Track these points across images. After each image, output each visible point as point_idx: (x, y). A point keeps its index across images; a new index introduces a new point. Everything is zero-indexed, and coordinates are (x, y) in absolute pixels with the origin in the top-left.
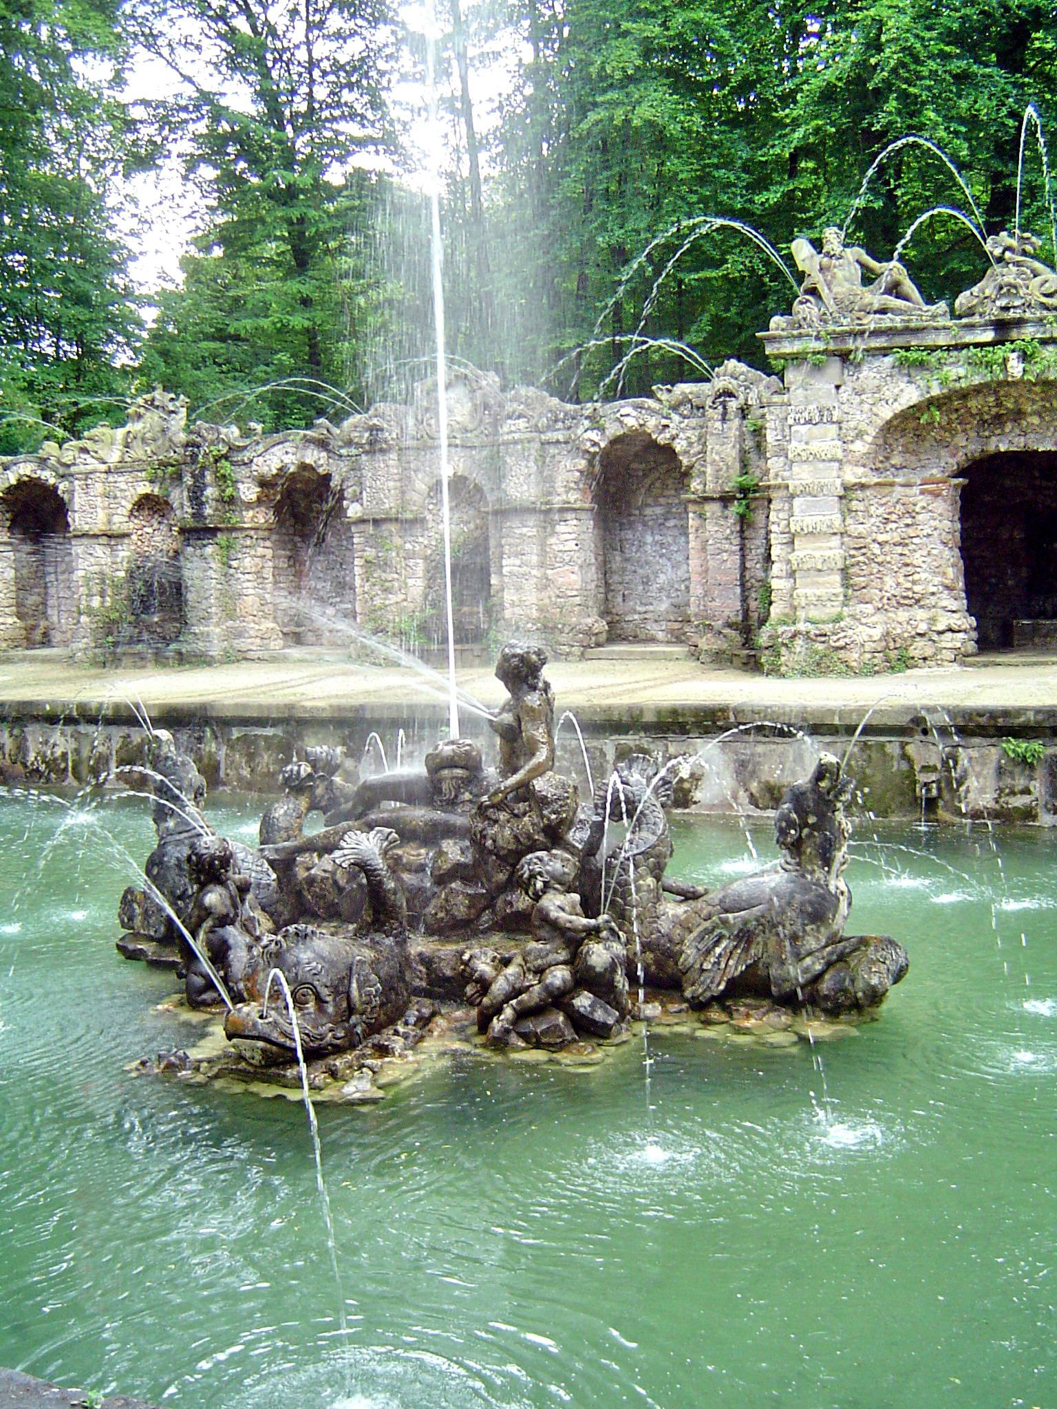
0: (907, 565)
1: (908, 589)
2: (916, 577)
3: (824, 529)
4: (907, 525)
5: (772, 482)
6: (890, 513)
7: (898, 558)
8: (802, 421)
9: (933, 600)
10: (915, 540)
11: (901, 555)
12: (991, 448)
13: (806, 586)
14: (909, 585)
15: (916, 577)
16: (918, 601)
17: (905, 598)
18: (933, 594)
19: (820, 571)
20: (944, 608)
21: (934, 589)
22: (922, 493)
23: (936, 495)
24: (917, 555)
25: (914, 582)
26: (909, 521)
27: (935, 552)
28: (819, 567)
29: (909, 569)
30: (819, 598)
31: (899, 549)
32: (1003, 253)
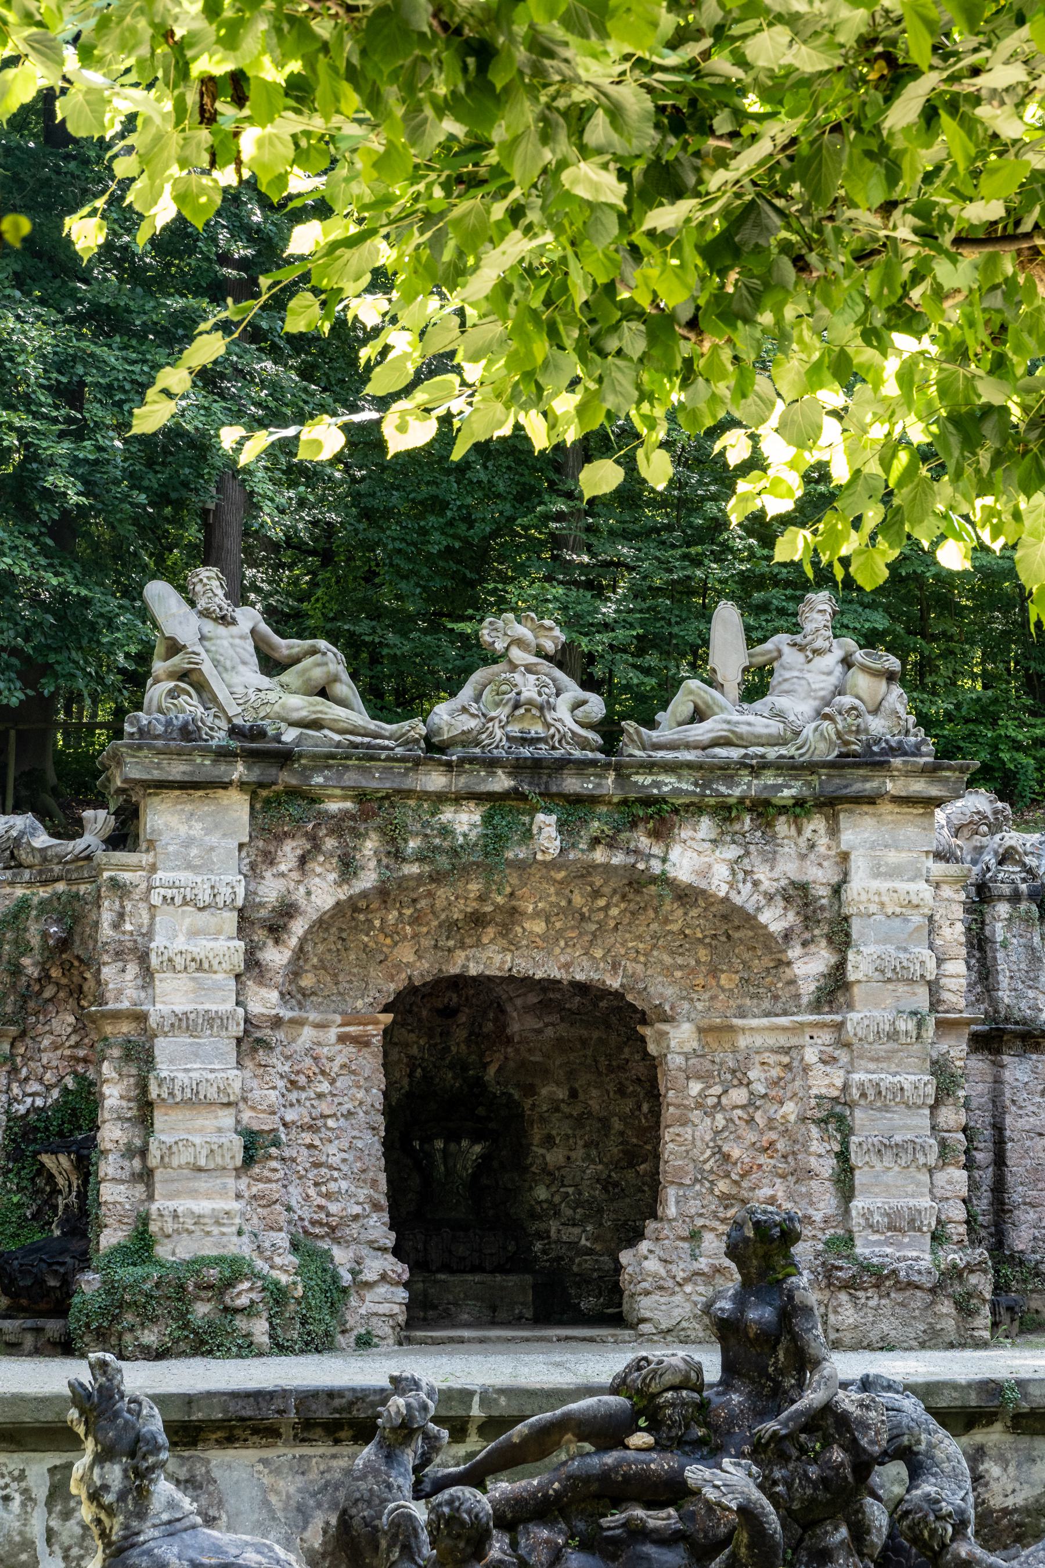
0: (316, 1165)
1: (320, 1207)
2: (333, 1186)
3: (212, 1093)
4: (320, 1096)
5: (111, 1006)
6: (298, 1073)
7: (305, 1152)
8: (178, 900)
9: (354, 1229)
10: (331, 1123)
11: (310, 1146)
12: (454, 970)
13: (170, 1197)
14: (323, 1202)
15: (333, 1186)
16: (333, 1229)
17: (313, 1223)
18: (356, 1217)
19: (200, 1170)
20: (370, 1243)
21: (357, 1210)
22: (342, 1039)
23: (361, 1042)
24: (332, 1149)
25: (328, 1196)
26: (325, 1087)
27: (360, 1144)
28: (202, 1162)
29: (323, 1171)
30: (198, 1219)
31: (307, 1137)
32: (507, 649)
